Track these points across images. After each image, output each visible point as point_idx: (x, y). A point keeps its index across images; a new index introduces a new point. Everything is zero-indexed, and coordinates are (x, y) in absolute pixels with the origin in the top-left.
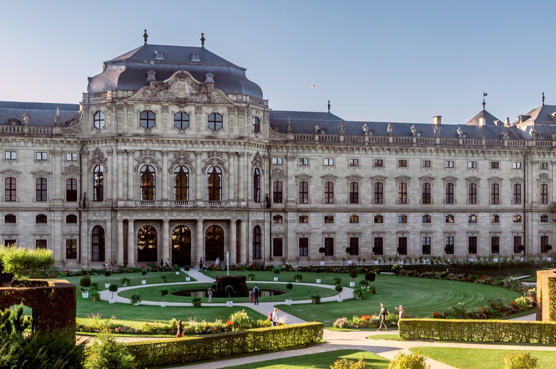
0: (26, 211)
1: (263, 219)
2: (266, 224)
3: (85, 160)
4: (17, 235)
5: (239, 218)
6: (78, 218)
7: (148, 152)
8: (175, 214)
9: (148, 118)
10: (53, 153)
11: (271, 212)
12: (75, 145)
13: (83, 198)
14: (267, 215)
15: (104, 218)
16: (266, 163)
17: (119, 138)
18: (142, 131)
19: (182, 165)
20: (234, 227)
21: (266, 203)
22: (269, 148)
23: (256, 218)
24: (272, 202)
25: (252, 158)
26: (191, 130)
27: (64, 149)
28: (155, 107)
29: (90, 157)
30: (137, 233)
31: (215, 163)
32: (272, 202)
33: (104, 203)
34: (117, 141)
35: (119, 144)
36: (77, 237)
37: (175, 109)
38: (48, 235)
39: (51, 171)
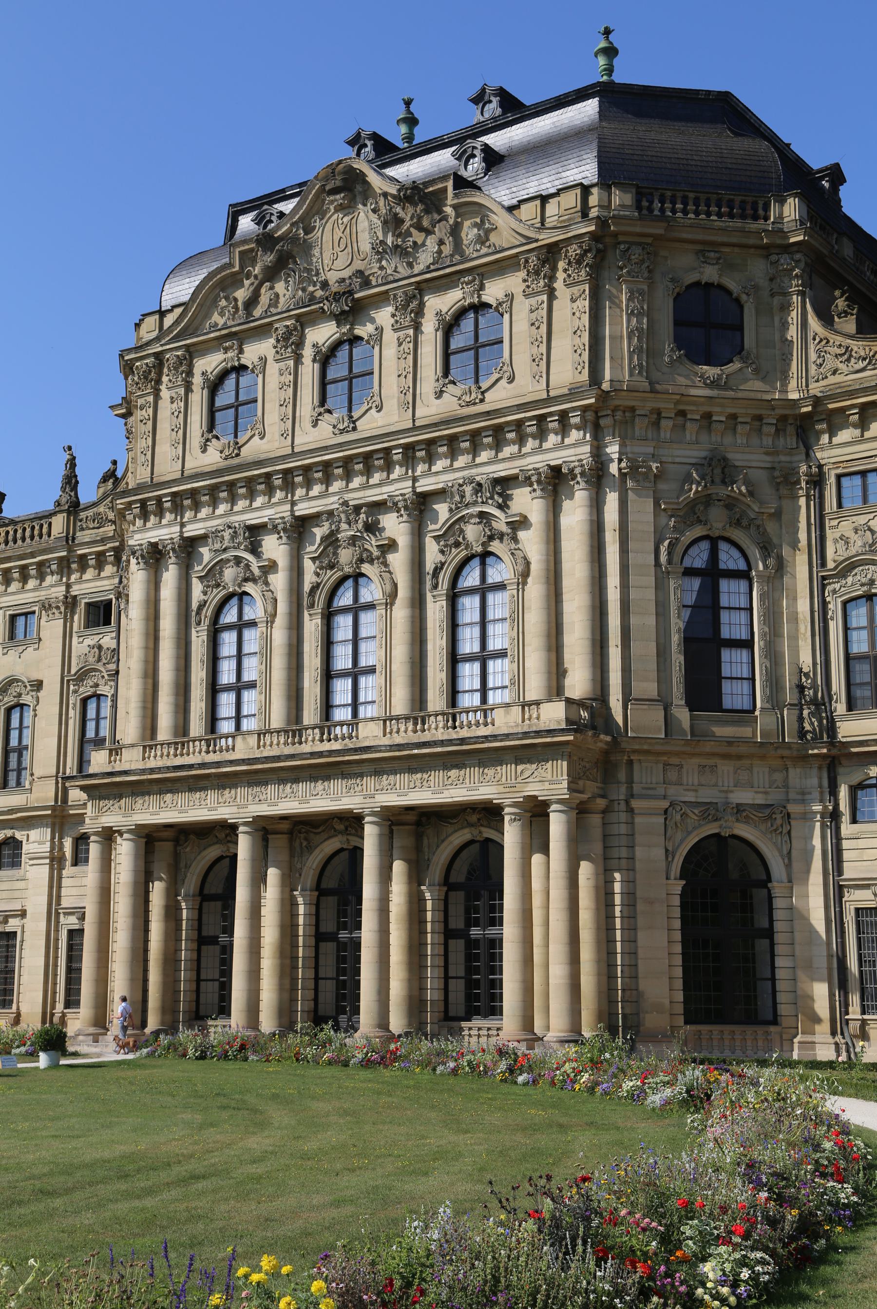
5: (534, 789)
7: (227, 535)
19: (348, 570)
20: (511, 837)
23: (707, 795)
24: (840, 708)
27: (75, 590)
31: (472, 532)
32: (840, 708)
39: (36, 676)
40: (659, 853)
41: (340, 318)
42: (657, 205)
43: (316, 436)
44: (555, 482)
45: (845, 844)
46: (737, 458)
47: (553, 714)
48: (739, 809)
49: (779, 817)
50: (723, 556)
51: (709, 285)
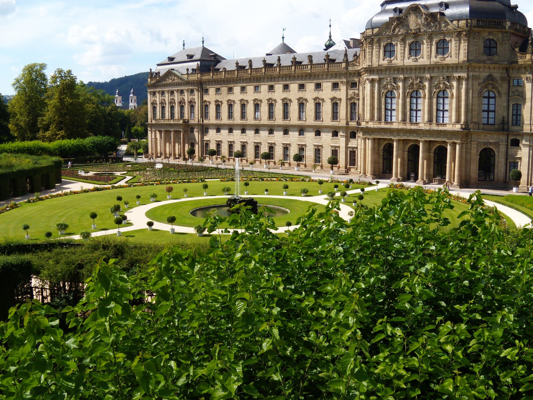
1: (497, 141)
2: (501, 147)
3: (361, 88)
7: (389, 79)
8: (401, 134)
9: (389, 51)
10: (342, 82)
11: (508, 135)
14: (503, 138)
16: (505, 85)
20: (449, 148)
21: (501, 126)
22: (507, 70)
23: (485, 141)
24: (510, 124)
25: (481, 81)
26: (423, 58)
27: (349, 79)
30: (382, 148)
32: (510, 124)
38: (339, 147)
40: (475, 151)
41: (414, 37)
42: (481, 23)
43: (409, 62)
44: (459, 79)
45: (509, 150)
46: (494, 75)
47: (458, 127)
48: (491, 143)
49: (497, 144)
50: (490, 94)
51: (490, 39)
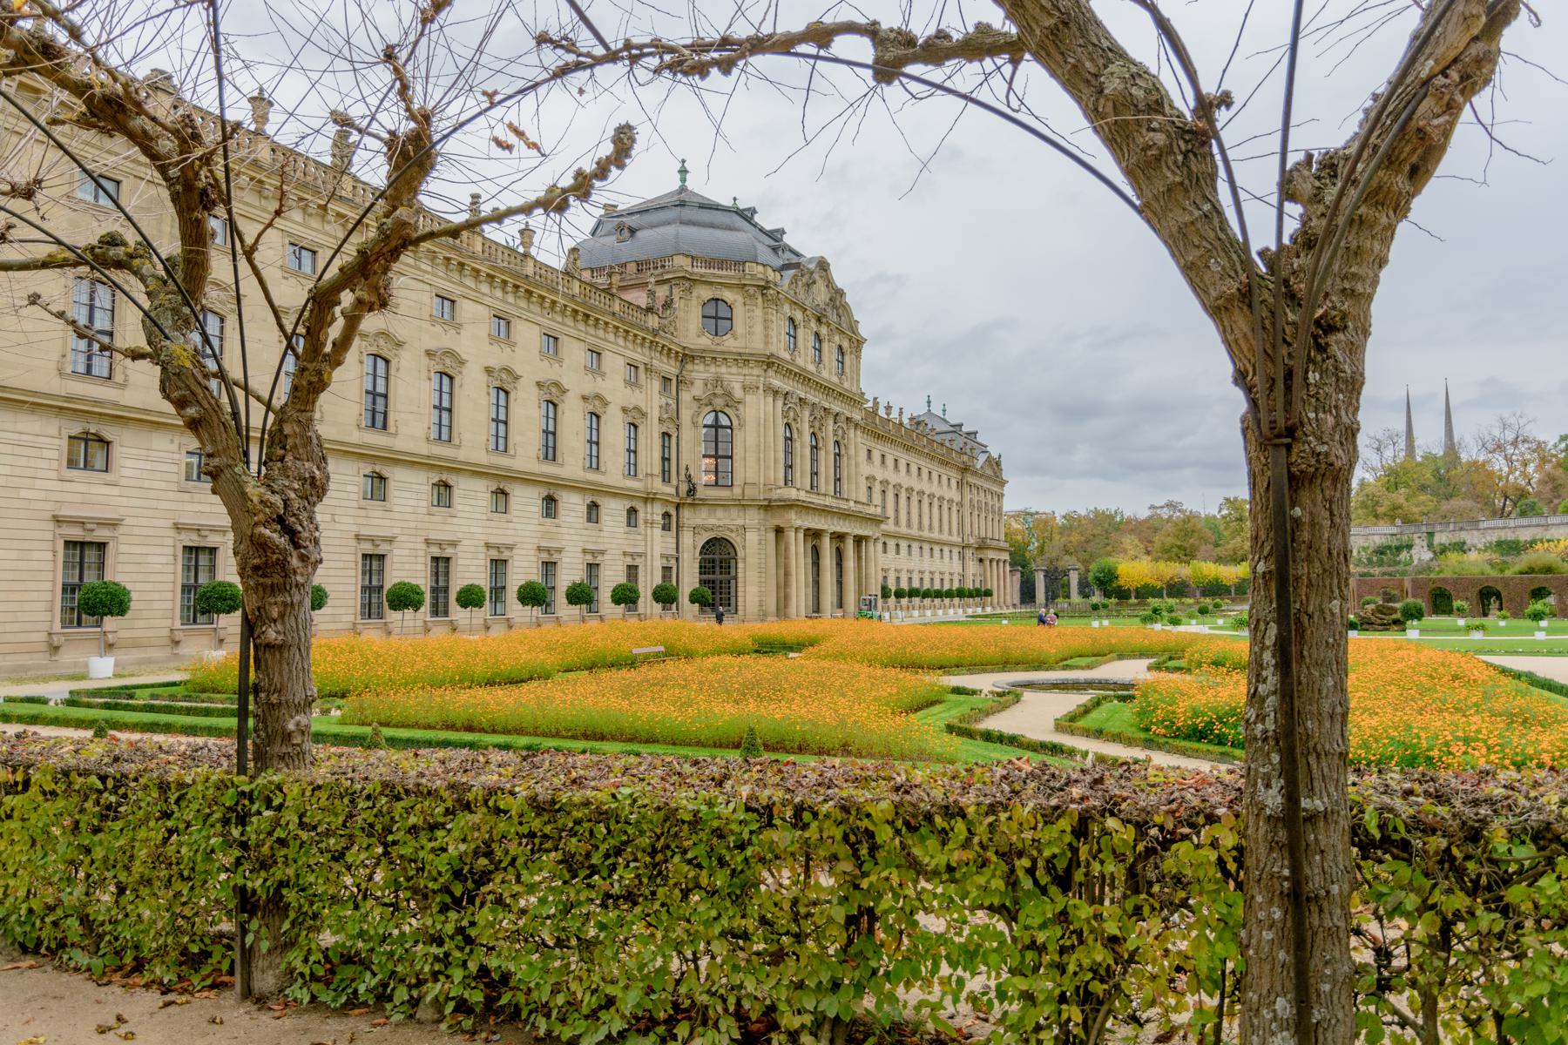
0: (615, 495)
3: (686, 396)
4: (602, 552)
6: (674, 519)
10: (649, 369)
12: (672, 362)
13: (682, 477)
15: (740, 522)
17: (769, 362)
18: (787, 356)
28: (798, 316)
29: (698, 390)
33: (737, 491)
34: (769, 365)
35: (771, 373)
36: (673, 563)
37: (813, 324)
